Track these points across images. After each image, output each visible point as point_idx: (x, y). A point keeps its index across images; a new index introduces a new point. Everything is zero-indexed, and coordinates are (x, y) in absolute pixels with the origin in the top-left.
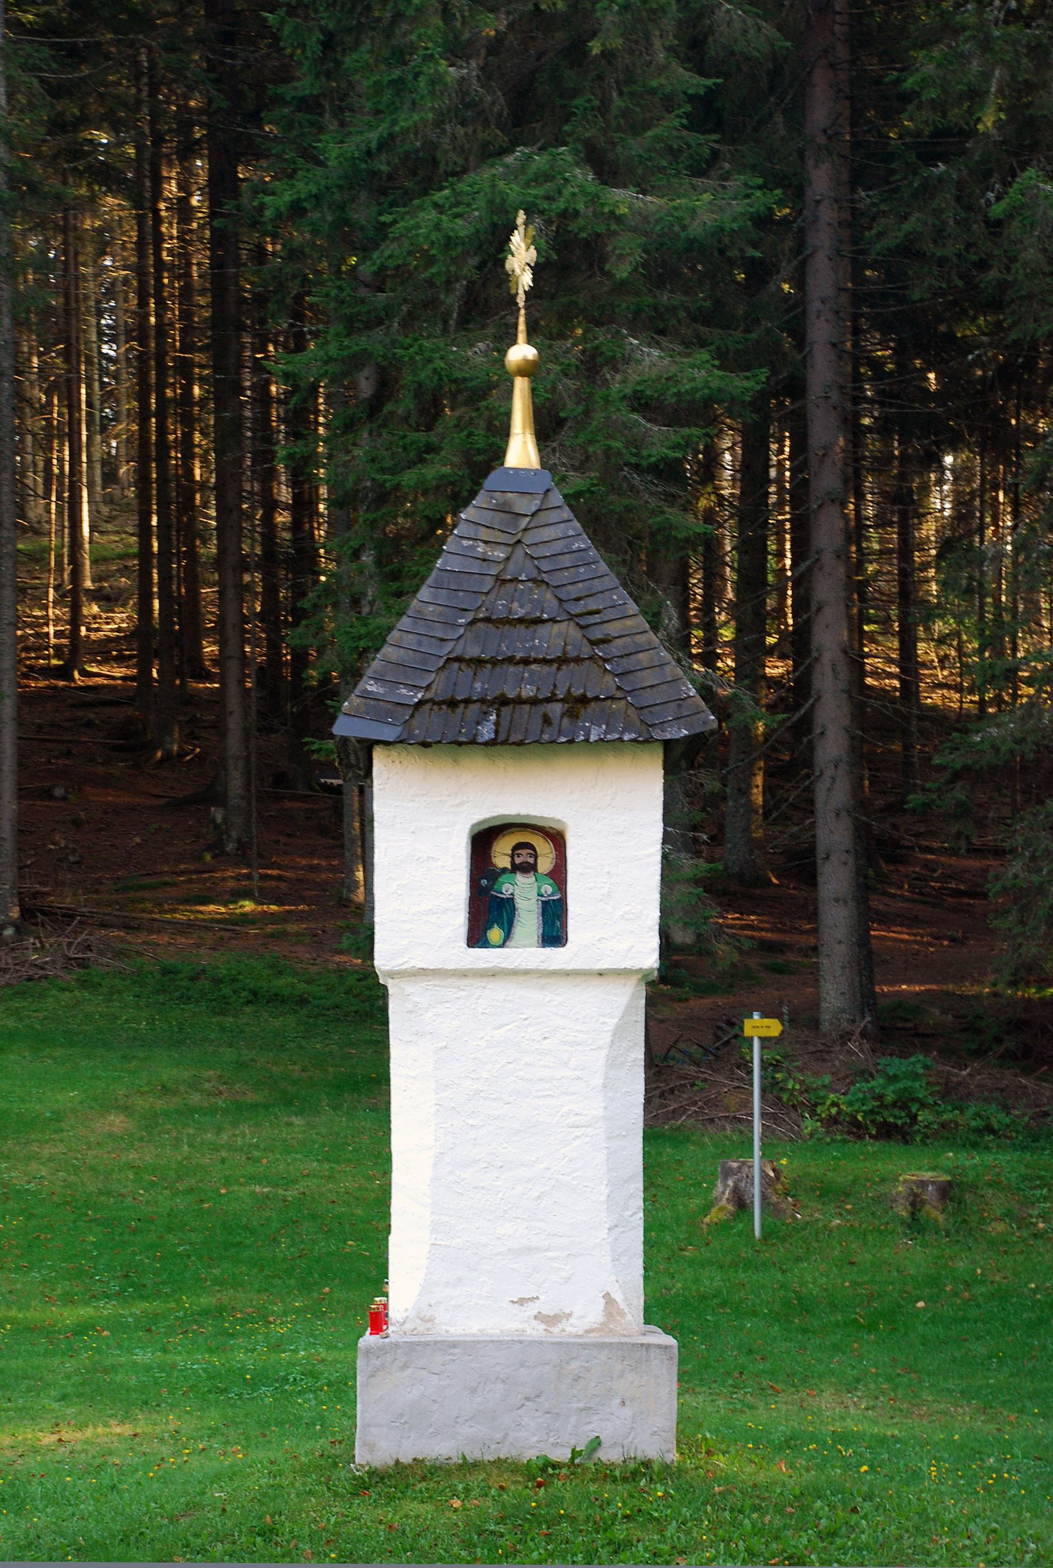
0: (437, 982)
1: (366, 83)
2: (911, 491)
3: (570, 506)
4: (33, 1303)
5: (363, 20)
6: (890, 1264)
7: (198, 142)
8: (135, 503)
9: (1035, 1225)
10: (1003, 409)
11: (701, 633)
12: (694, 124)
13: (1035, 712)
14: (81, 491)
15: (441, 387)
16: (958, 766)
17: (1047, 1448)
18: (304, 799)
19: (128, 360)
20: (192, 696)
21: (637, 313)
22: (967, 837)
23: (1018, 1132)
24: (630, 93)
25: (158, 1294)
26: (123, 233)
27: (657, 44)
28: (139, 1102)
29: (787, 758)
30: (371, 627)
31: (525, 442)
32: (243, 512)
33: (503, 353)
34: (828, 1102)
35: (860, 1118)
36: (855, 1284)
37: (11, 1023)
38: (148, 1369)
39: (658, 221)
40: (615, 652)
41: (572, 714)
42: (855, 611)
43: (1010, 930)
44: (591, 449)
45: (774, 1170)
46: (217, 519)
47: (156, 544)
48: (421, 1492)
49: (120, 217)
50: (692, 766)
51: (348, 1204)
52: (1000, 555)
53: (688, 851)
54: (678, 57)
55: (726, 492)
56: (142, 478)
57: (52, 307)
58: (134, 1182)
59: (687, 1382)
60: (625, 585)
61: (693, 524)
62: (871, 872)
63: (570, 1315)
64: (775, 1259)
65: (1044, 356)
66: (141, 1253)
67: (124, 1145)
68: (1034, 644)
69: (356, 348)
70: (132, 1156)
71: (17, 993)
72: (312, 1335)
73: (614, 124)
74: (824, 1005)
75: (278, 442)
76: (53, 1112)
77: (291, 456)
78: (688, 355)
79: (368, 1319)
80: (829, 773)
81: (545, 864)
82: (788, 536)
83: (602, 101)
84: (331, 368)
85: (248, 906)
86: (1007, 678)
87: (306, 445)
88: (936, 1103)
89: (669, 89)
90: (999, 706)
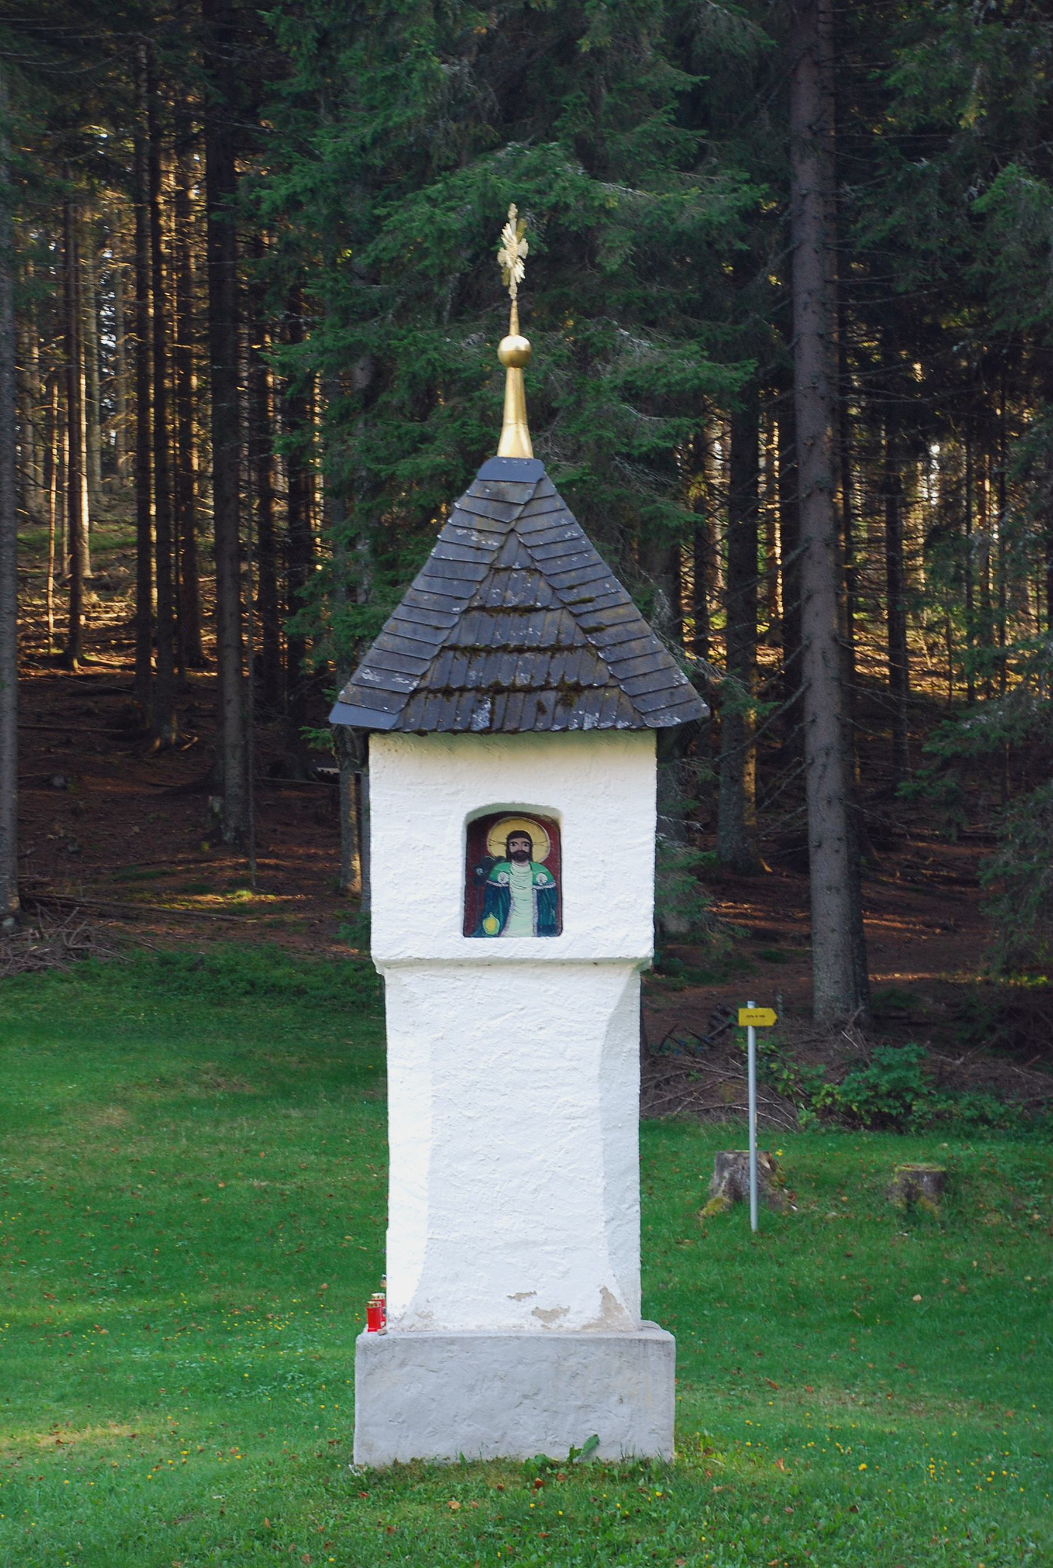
0: (432, 972)
1: (360, 79)
2: (898, 480)
3: (563, 496)
4: (32, 1301)
5: (357, 18)
6: (886, 1257)
7: (196, 136)
8: (134, 492)
9: (1030, 1216)
10: (988, 399)
11: (692, 622)
12: (683, 120)
13: (1023, 699)
14: (80, 480)
15: (435, 378)
16: (948, 753)
17: (1045, 1444)
18: (299, 787)
19: (127, 350)
20: (190, 685)
21: (627, 305)
22: (958, 825)
23: (1012, 1122)
24: (619, 90)
25: (156, 1291)
26: (123, 226)
27: (645, 42)
28: (138, 1095)
29: (779, 746)
30: (367, 616)
31: (518, 432)
32: (240, 502)
33: (496, 344)
34: (823, 1093)
35: (854, 1108)
36: (851, 1277)
37: (10, 1015)
38: (146, 1368)
39: (647, 215)
40: (608, 640)
41: (566, 703)
42: (845, 599)
43: (1002, 918)
44: (582, 439)
45: (770, 1162)
46: (215, 508)
47: (154, 534)
48: (419, 1493)
49: (120, 211)
50: (684, 754)
51: (345, 1197)
52: (987, 544)
53: (682, 839)
54: (666, 55)
55: (715, 482)
56: (141, 468)
57: (52, 298)
58: (132, 1176)
59: (685, 1378)
60: (617, 574)
61: (683, 513)
62: (863, 860)
63: (567, 1310)
64: (772, 1252)
65: (1028, 347)
66: (139, 1248)
67: (122, 1139)
68: (1021, 632)
69: (351, 340)
70: (131, 1149)
71: (16, 984)
72: (310, 1333)
73: (603, 119)
74: (818, 994)
75: (275, 432)
76: (51, 1105)
77: (287, 446)
78: (677, 346)
79: (366, 1315)
80: (820, 760)
81: (540, 853)
82: (777, 525)
83: (591, 97)
84: (326, 359)
85: (246, 895)
86: (995, 666)
87: (302, 436)
88: (930, 1093)
89: (657, 86)
90: (988, 694)
